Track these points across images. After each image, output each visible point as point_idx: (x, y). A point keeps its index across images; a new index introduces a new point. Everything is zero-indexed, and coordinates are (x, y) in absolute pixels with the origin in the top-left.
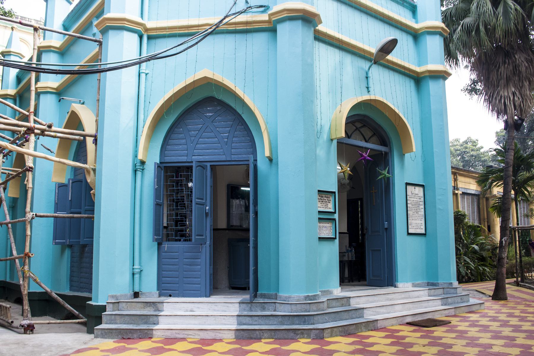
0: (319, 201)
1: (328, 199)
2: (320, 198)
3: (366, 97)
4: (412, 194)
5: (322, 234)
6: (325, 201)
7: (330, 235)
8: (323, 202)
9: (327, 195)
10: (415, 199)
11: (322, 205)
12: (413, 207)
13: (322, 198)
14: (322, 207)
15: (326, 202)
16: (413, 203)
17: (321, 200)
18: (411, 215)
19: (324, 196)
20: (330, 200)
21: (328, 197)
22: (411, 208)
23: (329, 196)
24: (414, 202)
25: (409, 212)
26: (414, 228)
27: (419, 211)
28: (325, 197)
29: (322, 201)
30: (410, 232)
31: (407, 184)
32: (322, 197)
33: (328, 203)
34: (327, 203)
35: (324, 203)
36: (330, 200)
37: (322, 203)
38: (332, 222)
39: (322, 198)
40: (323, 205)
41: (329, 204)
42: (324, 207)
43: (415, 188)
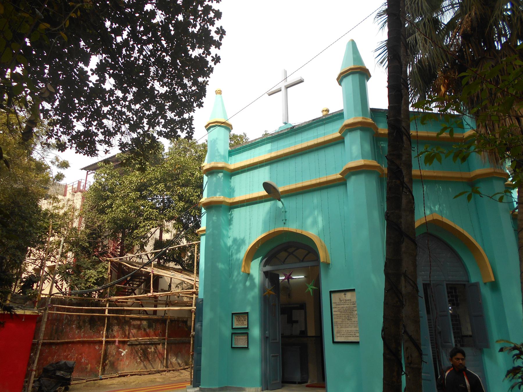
2: (237, 318)
3: (281, 228)
4: (340, 300)
10: (345, 306)
12: (343, 314)
16: (342, 310)
17: (238, 320)
18: (339, 323)
21: (244, 317)
22: (339, 316)
24: (344, 308)
25: (334, 320)
26: (345, 336)
27: (352, 317)
28: (242, 317)
30: (336, 340)
31: (331, 292)
32: (240, 317)
41: (245, 322)
43: (345, 294)
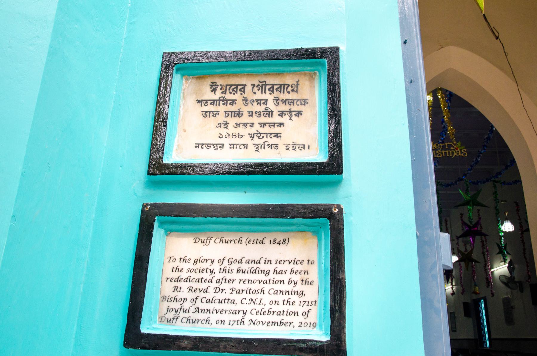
0: (206, 114)
1: (285, 96)
5: (214, 317)
6: (262, 108)
7: (296, 320)
8: (239, 114)
9: (279, 74)
11: (231, 129)
13: (229, 96)
14: (227, 142)
15: (268, 113)
17: (222, 108)
19: (248, 82)
20: (305, 102)
21: (282, 88)
23: (289, 80)
28: (262, 87)
29: (227, 114)
33: (285, 119)
34: (276, 119)
35: (245, 119)
36: (305, 102)
37: (232, 121)
38: (316, 233)
39: (229, 96)
40: (241, 130)
42: (246, 140)
